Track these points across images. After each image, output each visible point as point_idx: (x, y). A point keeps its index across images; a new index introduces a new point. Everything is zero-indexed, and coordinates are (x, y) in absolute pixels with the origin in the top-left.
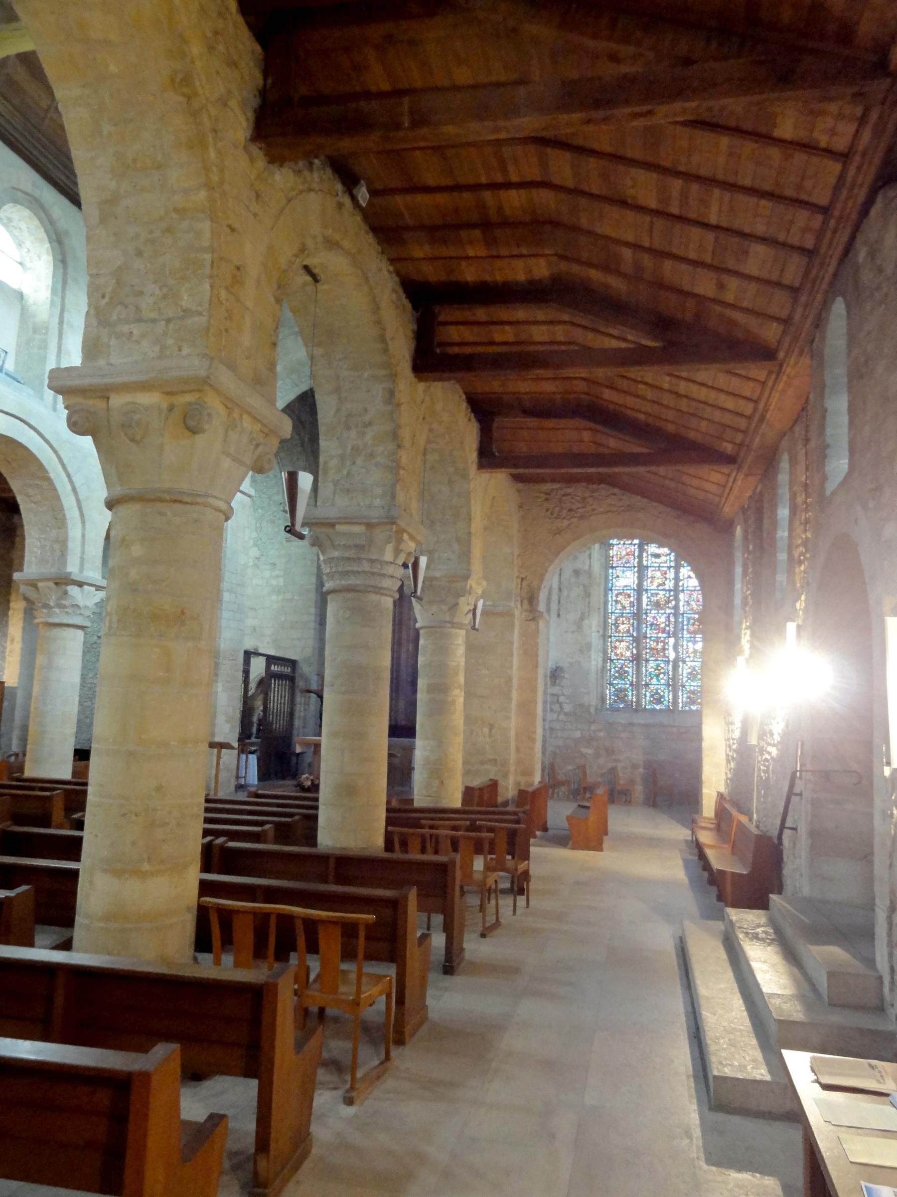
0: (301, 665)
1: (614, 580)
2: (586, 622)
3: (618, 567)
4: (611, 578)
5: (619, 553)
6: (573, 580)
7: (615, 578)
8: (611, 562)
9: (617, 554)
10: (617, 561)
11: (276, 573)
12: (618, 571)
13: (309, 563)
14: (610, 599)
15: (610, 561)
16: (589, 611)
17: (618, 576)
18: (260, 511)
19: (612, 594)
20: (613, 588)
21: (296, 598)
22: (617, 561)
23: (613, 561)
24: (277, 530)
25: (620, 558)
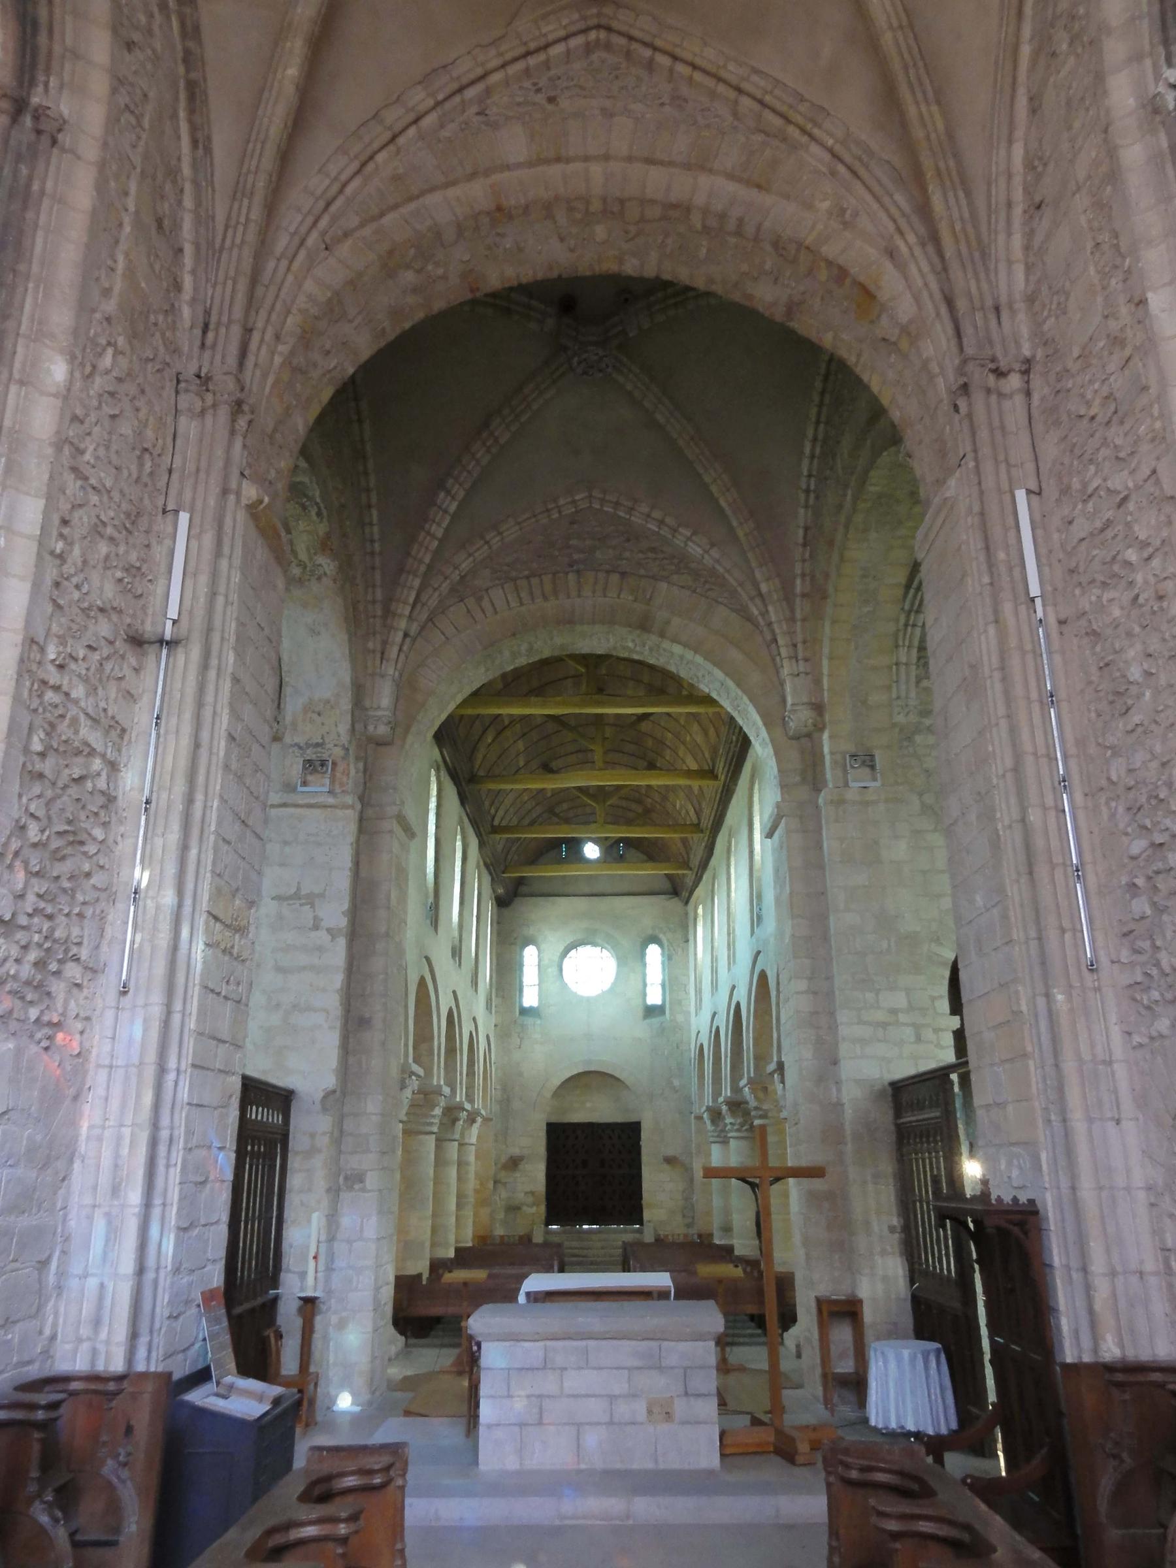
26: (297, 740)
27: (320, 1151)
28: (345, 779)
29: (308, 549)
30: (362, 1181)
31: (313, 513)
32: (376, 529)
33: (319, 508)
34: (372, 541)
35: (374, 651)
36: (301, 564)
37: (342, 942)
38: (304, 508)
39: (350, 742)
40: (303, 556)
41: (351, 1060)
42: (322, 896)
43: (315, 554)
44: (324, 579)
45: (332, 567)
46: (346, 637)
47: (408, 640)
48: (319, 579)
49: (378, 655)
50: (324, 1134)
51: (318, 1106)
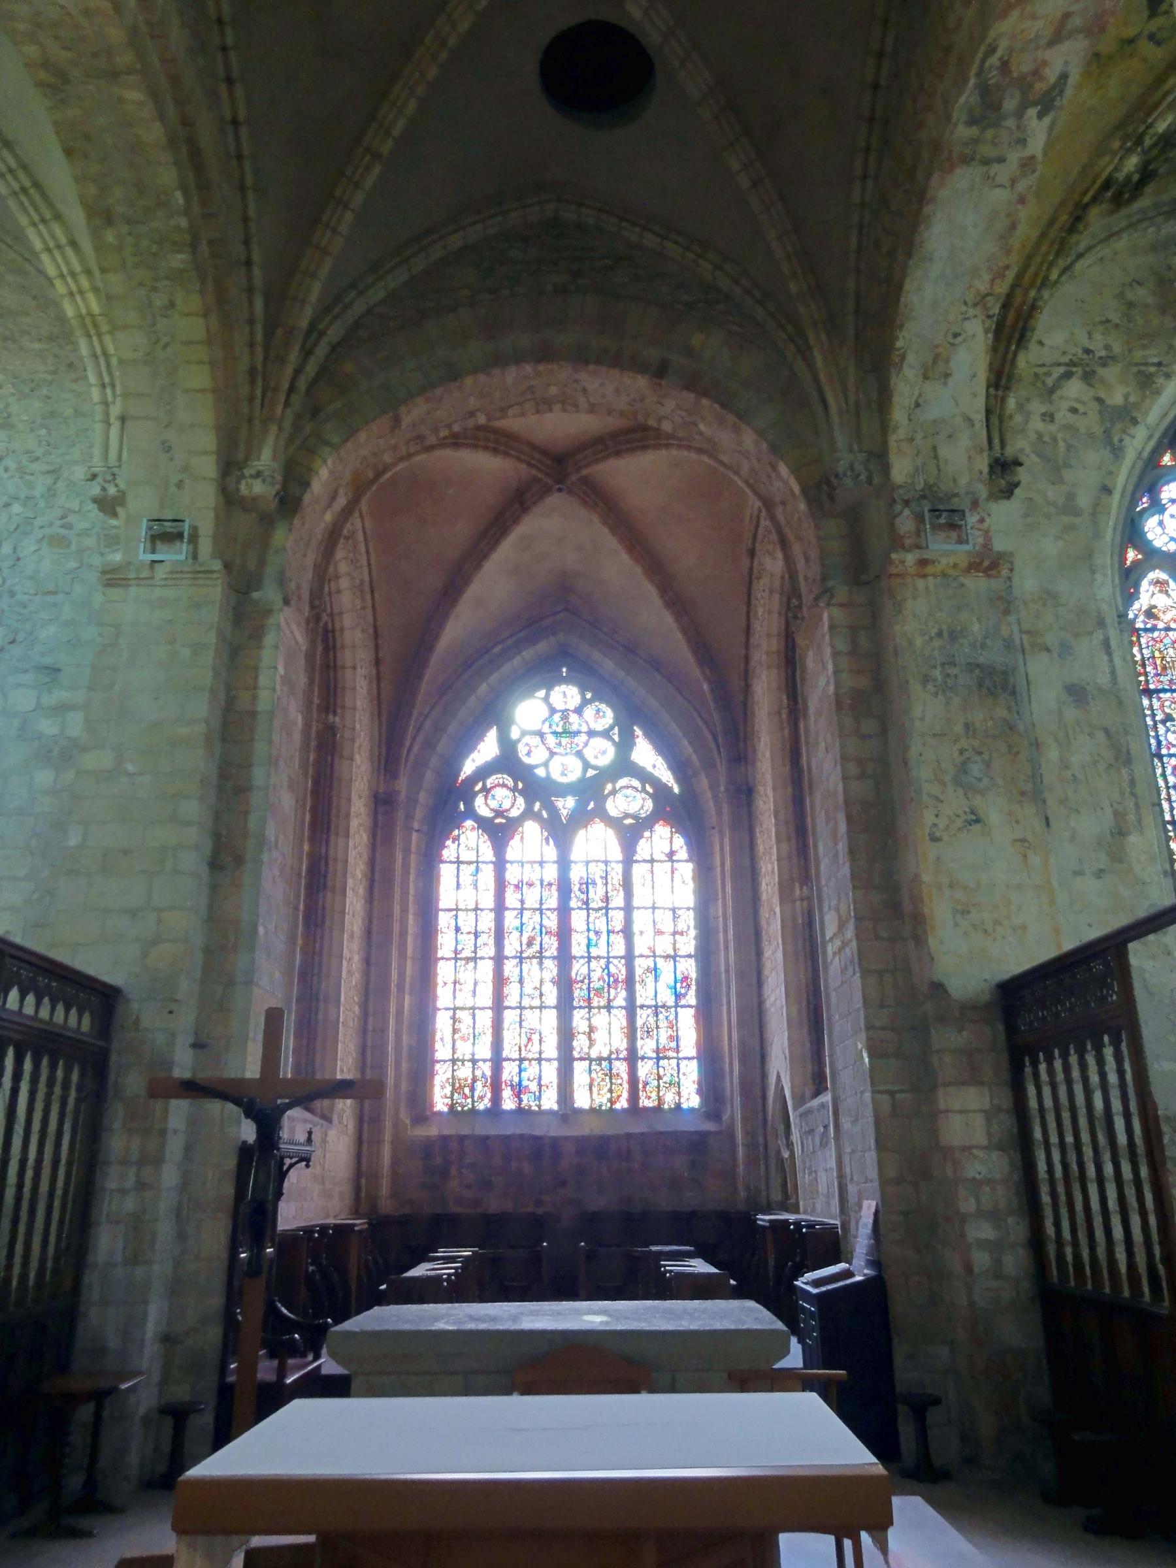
0: (135, 1006)
1: (1161, 729)
2: (1133, 839)
3: (1164, 691)
4: (1149, 721)
5: (1157, 654)
6: (1071, 714)
7: (1164, 722)
8: (1142, 678)
9: (1154, 657)
10: (1157, 675)
11: (60, 695)
12: (1167, 704)
13: (186, 652)
14: (1161, 783)
15: (1140, 674)
16: (1137, 805)
17: (1168, 718)
18: (16, 508)
19: (1164, 768)
20: (1164, 751)
21: (130, 768)
22: (1157, 675)
23: (1146, 674)
24: (74, 565)
25: (1164, 668)
31: (999, 53)
33: (983, 61)
38: (1005, 66)
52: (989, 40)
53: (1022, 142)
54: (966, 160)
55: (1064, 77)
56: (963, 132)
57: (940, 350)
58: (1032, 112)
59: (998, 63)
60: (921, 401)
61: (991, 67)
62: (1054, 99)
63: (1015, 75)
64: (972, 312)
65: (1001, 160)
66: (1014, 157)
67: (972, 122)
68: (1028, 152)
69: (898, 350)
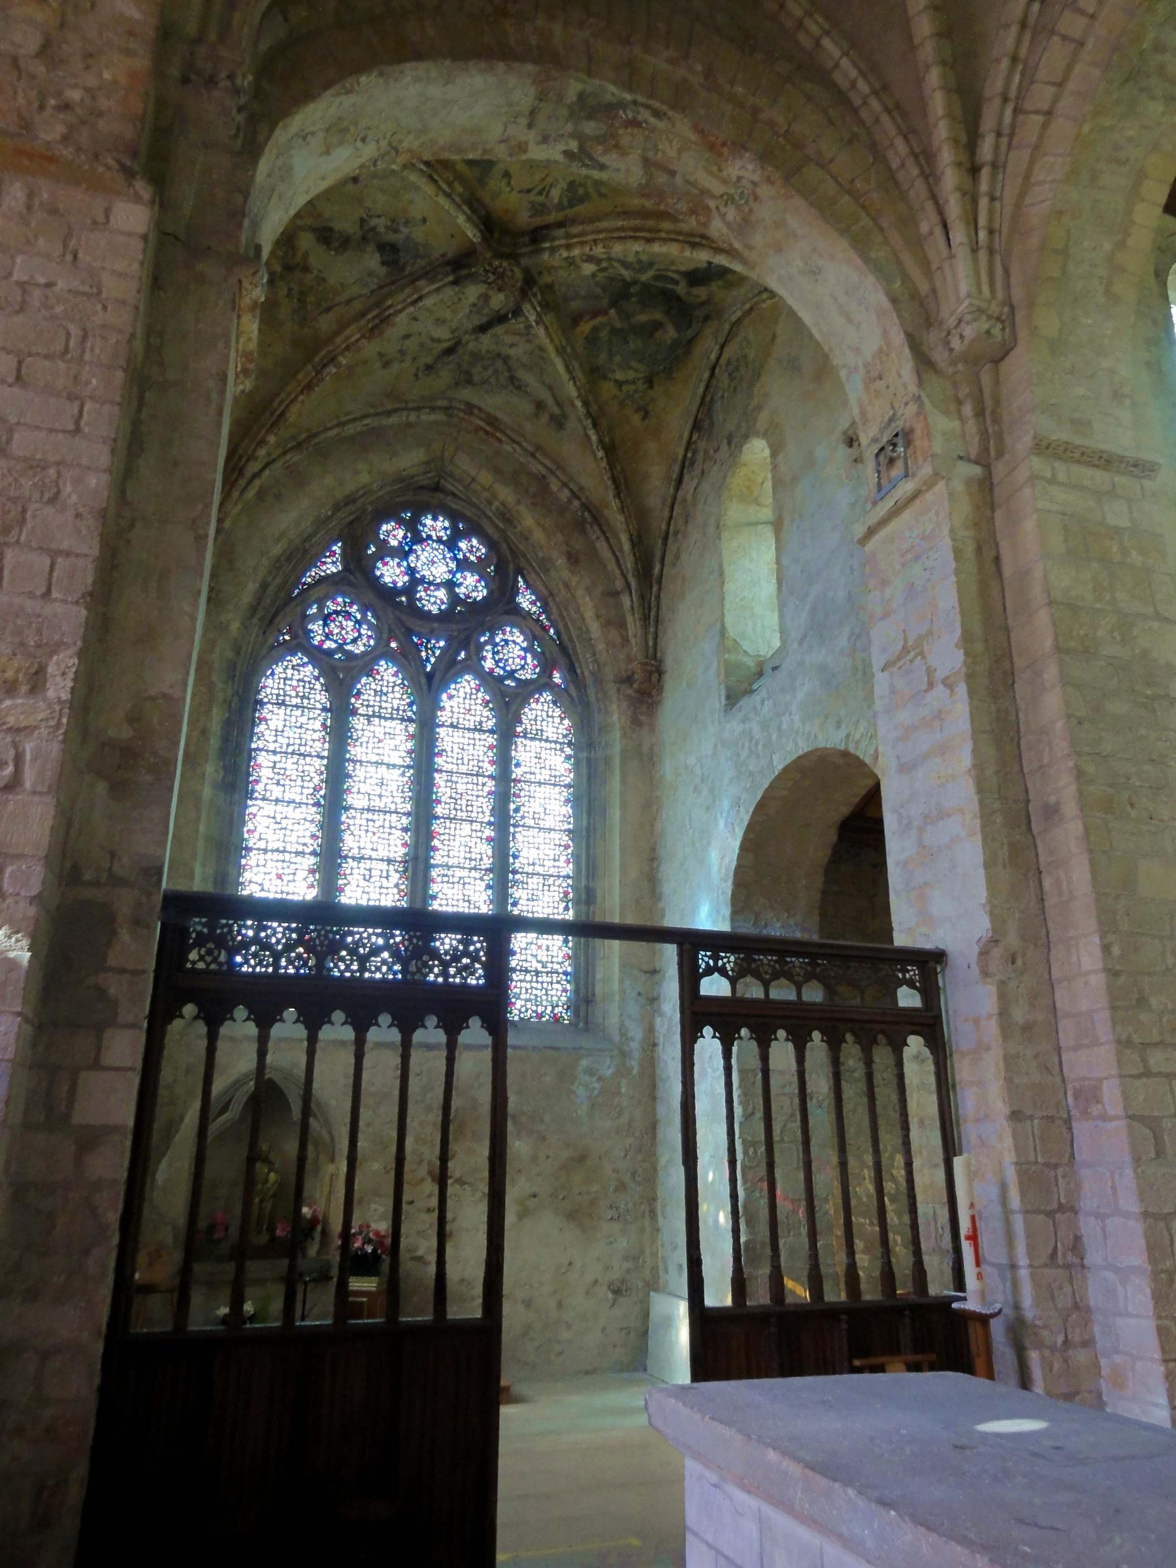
26: (871, 435)
27: (988, 1049)
28: (926, 443)
29: (711, 173)
30: (1098, 1100)
31: (652, 120)
32: (845, 62)
33: (648, 107)
34: (853, 84)
35: (931, 233)
36: (729, 199)
37: (962, 689)
39: (921, 383)
40: (717, 188)
41: (1047, 883)
42: (930, 633)
43: (720, 170)
44: (759, 191)
45: (750, 167)
46: (844, 244)
47: (985, 174)
48: (756, 198)
49: (938, 231)
50: (989, 1017)
51: (975, 972)
52: (670, 113)
53: (545, 139)
54: (541, 97)
55: (603, 167)
56: (573, 88)
57: (352, 129)
58: (574, 145)
59: (640, 118)
60: (309, 137)
61: (639, 113)
62: (581, 160)
63: (621, 132)
64: (384, 143)
65: (530, 126)
66: (531, 136)
67: (581, 96)
68: (531, 146)
69: (359, 84)
